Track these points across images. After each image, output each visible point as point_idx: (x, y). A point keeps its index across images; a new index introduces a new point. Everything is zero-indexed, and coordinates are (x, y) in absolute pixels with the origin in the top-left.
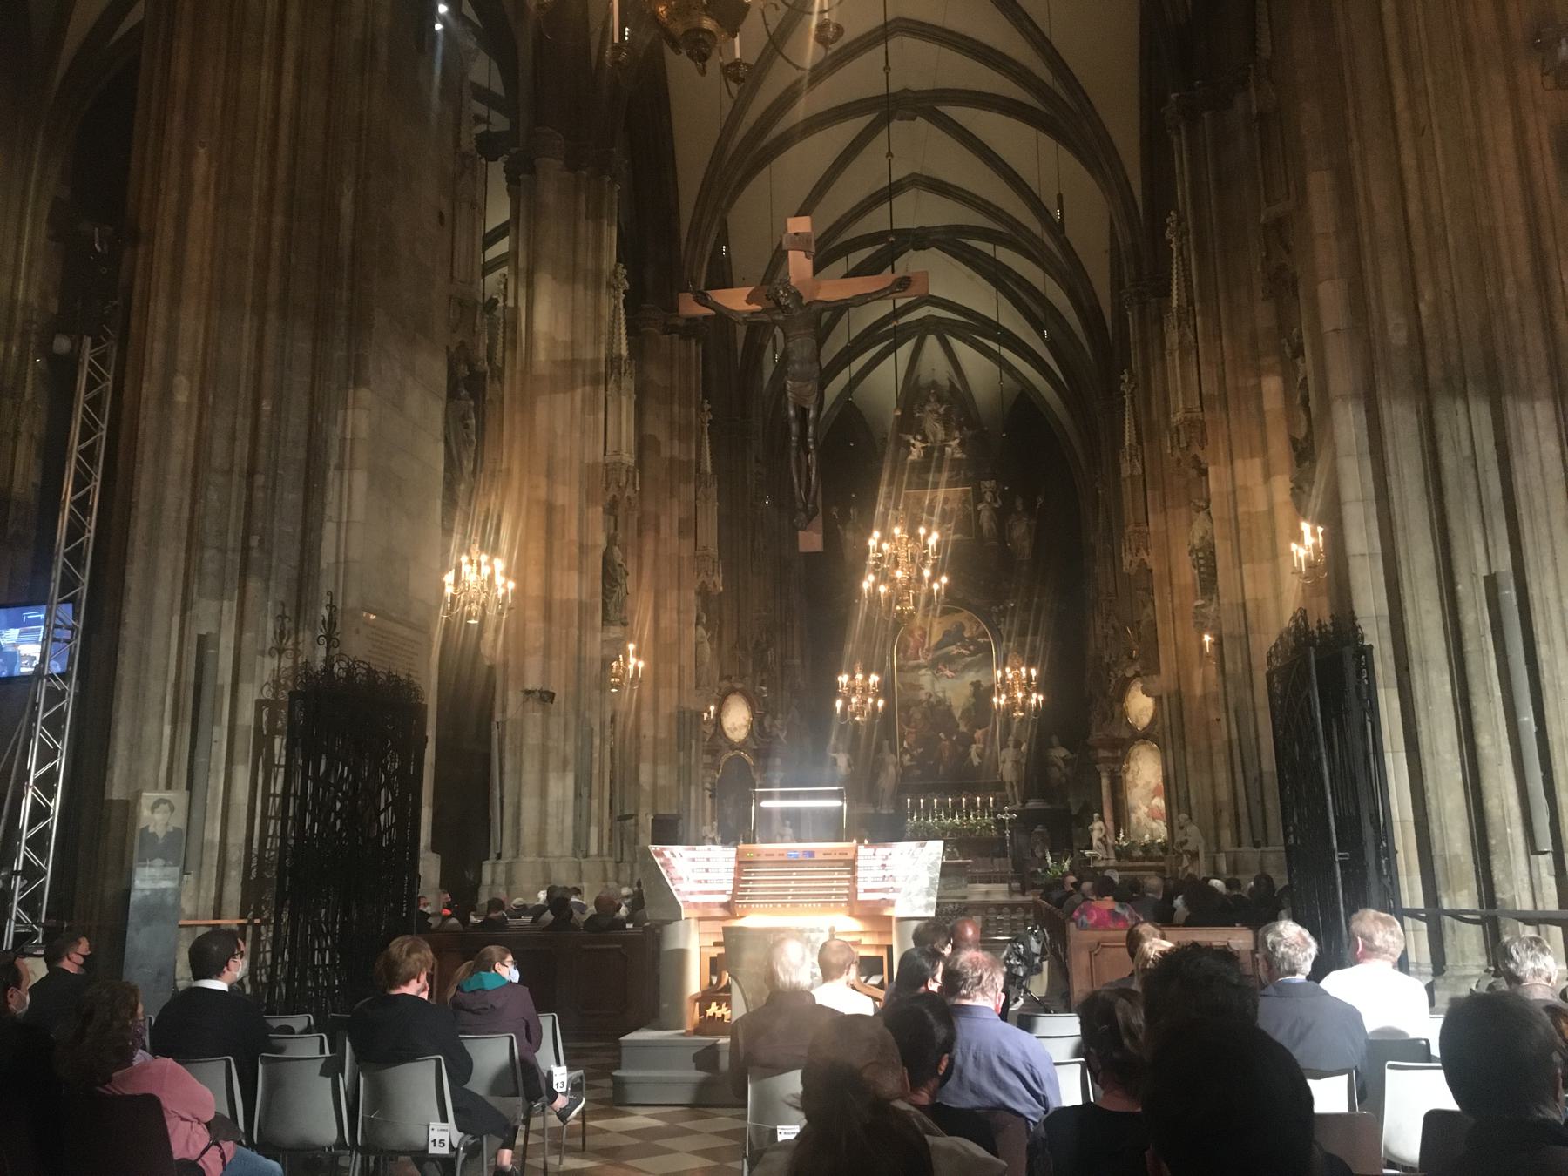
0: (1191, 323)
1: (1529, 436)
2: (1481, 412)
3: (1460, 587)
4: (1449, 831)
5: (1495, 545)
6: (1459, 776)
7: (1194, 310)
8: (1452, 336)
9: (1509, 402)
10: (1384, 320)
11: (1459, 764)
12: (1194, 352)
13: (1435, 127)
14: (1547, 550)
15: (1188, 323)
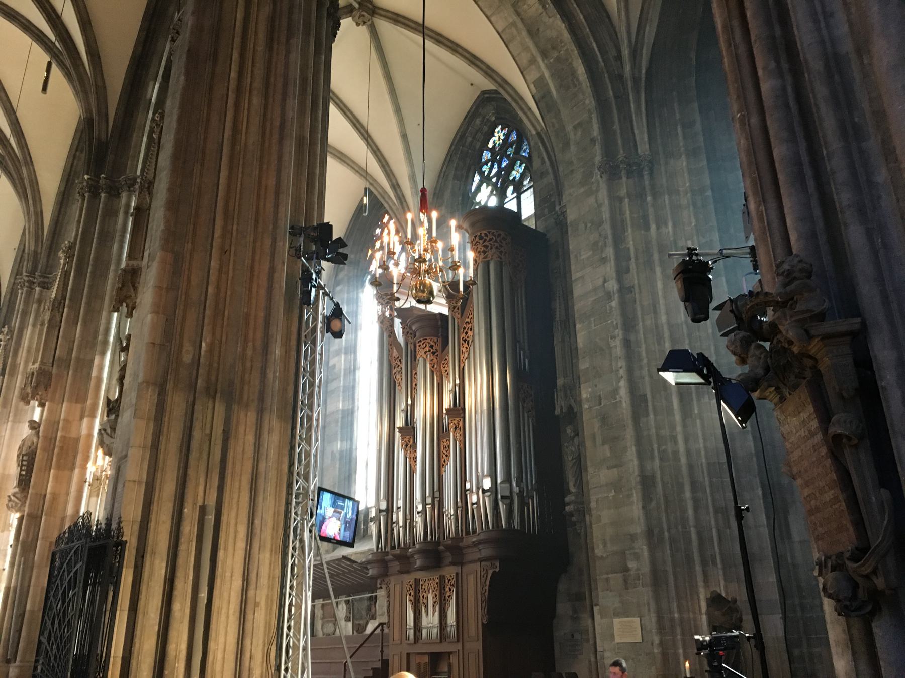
0: (61, 310)
1: (241, 429)
2: (220, 409)
3: (185, 510)
4: (142, 665)
5: (210, 489)
6: (157, 628)
7: (64, 304)
8: (215, 365)
9: (235, 407)
10: (181, 345)
11: (158, 620)
12: (58, 328)
13: (232, 252)
14: (236, 496)
15: (59, 310)
